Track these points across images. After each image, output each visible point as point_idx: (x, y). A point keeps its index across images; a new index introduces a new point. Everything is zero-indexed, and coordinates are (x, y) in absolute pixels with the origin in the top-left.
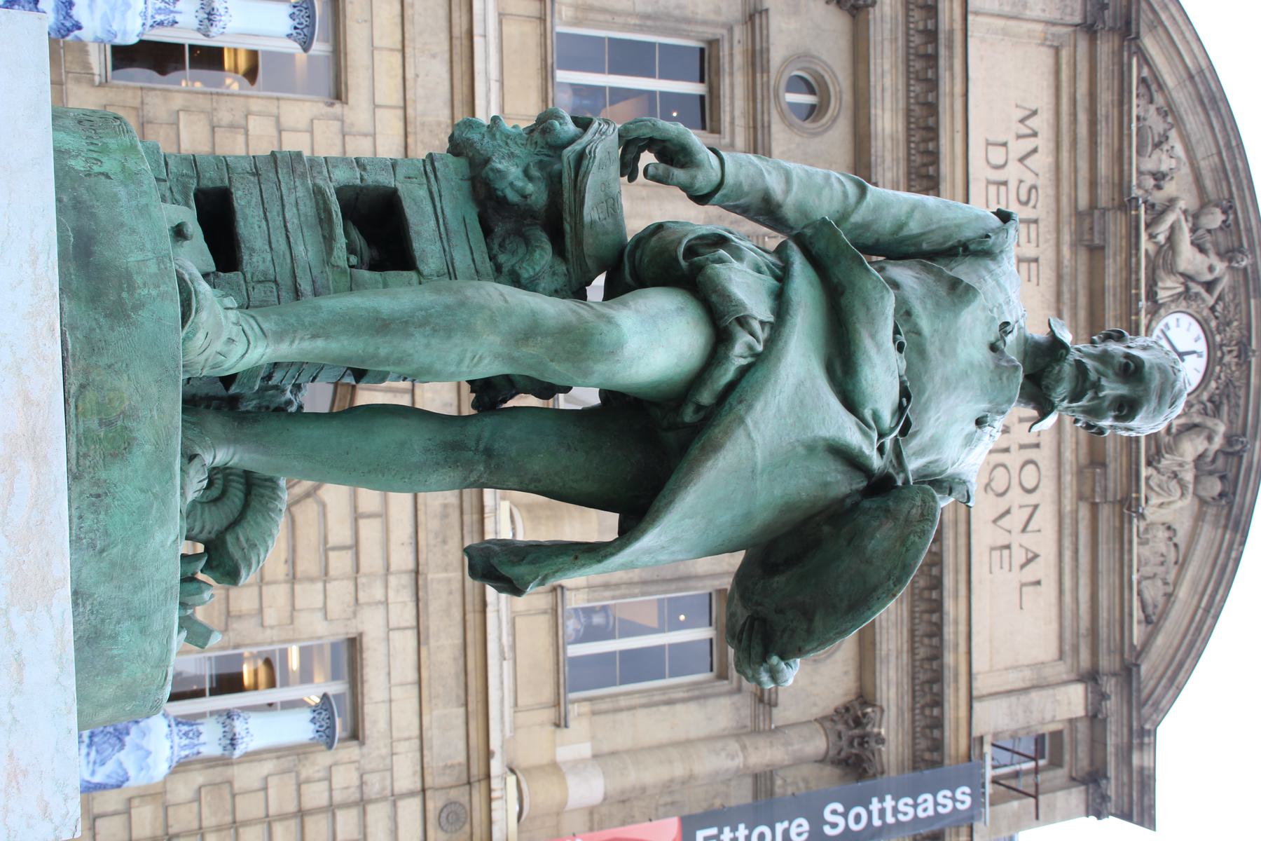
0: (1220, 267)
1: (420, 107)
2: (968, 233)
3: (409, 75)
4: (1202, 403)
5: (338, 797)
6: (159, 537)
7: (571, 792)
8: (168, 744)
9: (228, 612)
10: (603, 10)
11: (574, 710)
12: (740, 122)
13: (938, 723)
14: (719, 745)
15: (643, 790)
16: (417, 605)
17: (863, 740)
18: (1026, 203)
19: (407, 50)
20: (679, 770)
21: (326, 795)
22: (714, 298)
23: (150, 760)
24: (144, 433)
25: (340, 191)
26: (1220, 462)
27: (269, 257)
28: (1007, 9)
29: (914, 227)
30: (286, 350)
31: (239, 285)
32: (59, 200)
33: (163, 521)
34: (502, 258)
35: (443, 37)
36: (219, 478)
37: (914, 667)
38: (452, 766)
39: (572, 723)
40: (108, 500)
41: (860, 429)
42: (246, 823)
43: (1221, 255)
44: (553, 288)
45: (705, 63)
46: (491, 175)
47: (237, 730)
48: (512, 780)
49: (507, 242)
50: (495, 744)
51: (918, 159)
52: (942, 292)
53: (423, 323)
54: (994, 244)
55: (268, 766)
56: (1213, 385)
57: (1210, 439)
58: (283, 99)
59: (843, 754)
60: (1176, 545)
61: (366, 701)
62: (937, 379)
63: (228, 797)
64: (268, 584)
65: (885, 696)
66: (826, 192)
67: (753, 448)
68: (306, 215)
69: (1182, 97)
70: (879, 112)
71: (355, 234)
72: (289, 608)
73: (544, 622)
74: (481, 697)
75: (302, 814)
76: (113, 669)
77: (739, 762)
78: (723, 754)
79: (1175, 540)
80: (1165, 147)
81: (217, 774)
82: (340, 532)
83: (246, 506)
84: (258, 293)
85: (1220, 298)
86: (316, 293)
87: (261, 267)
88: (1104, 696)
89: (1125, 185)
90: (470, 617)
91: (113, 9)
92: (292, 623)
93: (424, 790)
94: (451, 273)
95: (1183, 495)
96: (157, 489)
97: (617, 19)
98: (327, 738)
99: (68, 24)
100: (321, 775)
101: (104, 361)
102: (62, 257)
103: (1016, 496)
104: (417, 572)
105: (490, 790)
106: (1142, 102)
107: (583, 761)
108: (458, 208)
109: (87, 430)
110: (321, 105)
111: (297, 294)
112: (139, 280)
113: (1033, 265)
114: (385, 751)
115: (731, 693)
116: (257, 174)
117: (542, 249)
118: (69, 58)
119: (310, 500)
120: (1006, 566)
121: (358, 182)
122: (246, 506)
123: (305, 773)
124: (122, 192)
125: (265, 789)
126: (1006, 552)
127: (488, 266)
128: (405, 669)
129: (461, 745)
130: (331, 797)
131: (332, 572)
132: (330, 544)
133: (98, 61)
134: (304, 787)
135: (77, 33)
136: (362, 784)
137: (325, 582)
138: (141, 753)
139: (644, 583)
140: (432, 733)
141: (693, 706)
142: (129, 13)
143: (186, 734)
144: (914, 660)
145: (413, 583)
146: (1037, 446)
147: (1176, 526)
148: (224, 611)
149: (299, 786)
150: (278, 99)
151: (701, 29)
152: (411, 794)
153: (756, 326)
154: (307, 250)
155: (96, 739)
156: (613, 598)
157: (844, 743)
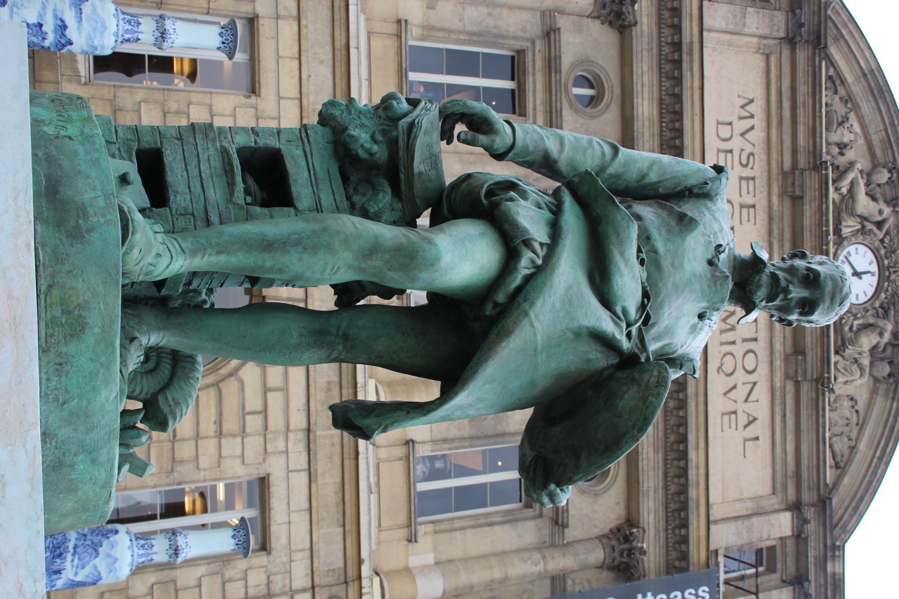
0: (887, 211)
1: (312, 98)
2: (692, 181)
3: (304, 76)
4: (875, 309)
6: (104, 394)
7: (419, 589)
8: (130, 553)
9: (174, 458)
10: (443, 30)
11: (422, 529)
12: (540, 108)
13: (685, 540)
14: (526, 555)
15: (472, 587)
16: (309, 454)
17: (630, 552)
18: (746, 166)
19: (303, 58)
20: (497, 574)
21: (243, 590)
22: (507, 226)
23: (117, 565)
24: (94, 319)
25: (239, 151)
26: (889, 351)
27: (189, 198)
28: (731, 27)
29: (653, 177)
30: (199, 263)
31: (167, 217)
32: (35, 155)
33: (107, 383)
34: (355, 198)
35: (329, 48)
36: (152, 353)
37: (667, 499)
38: (334, 570)
39: (420, 539)
40: (68, 367)
41: (613, 320)
43: (887, 203)
44: (392, 220)
45: (515, 66)
46: (348, 139)
47: (179, 543)
48: (376, 580)
49: (359, 187)
50: (364, 554)
51: (668, 134)
52: (673, 222)
53: (297, 243)
54: (711, 189)
55: (202, 570)
56: (883, 295)
57: (881, 335)
58: (215, 93)
59: (616, 563)
60: (857, 412)
61: (272, 523)
62: (669, 285)
63: (173, 592)
64: (202, 438)
65: (646, 520)
66: (589, 151)
67: (535, 334)
68: (215, 168)
69: (858, 90)
70: (640, 101)
71: (251, 181)
72: (217, 456)
73: (400, 466)
74: (354, 520)
76: (72, 489)
77: (540, 567)
78: (529, 562)
79: (857, 408)
80: (846, 125)
81: (165, 575)
82: (254, 402)
83: (173, 375)
84: (180, 223)
85: (887, 233)
86: (221, 223)
87: (183, 204)
88: (806, 521)
89: (818, 152)
90: (346, 462)
91: (95, 30)
92: (219, 466)
93: (313, 587)
94: (319, 209)
95: (861, 375)
96: (103, 359)
97: (452, 36)
98: (244, 549)
99: (63, 41)
100: (239, 576)
101: (66, 268)
102: (36, 194)
103: (740, 376)
104: (309, 430)
105: (361, 588)
106: (830, 93)
107: (428, 566)
108: (323, 162)
109: (53, 317)
110: (242, 97)
111: (208, 223)
112: (91, 211)
113: (752, 210)
114: (285, 559)
115: (534, 518)
116: (180, 138)
117: (384, 192)
118: (64, 65)
119: (233, 378)
120: (733, 426)
121: (253, 144)
122: (173, 375)
124: (81, 150)
125: (199, 586)
126: (733, 416)
127: (345, 204)
128: (300, 500)
130: (246, 592)
131: (248, 430)
132: (247, 410)
133: (84, 67)
134: (227, 585)
135: (69, 47)
136: (269, 582)
137: (243, 437)
138: (110, 559)
139: (472, 438)
140: (319, 546)
141: (507, 527)
142: (106, 33)
143: (143, 546)
144: (667, 495)
145: (306, 437)
146: (755, 340)
147: (857, 398)
148: (171, 458)
149: (224, 584)
150: (211, 93)
151: (512, 42)
152: (304, 590)
153: (537, 246)
154: (215, 193)
155: (78, 550)
156: (450, 449)
157: (616, 554)
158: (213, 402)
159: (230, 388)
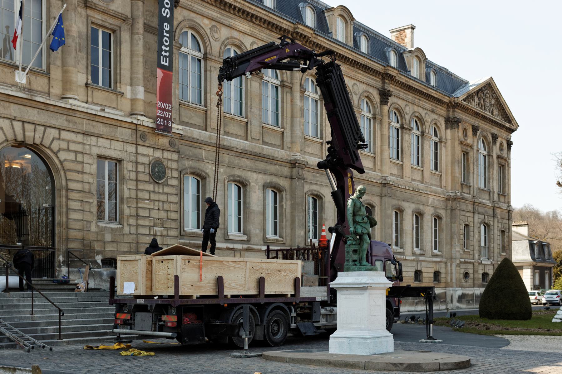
5: (134, 169)
14: (135, 42)
42: (137, 196)
75: (137, 180)
82: (72, 156)
90: (97, 120)
123: (128, 178)
128: (106, 143)
129: (127, 130)
136: (132, 162)
149: (130, 180)
158: (71, 173)
159: (67, 165)
